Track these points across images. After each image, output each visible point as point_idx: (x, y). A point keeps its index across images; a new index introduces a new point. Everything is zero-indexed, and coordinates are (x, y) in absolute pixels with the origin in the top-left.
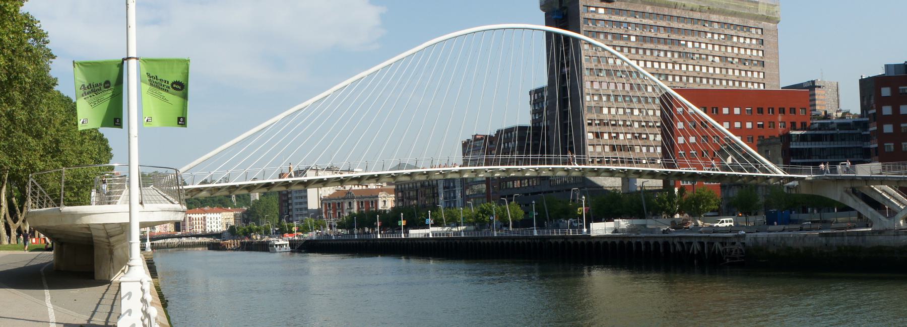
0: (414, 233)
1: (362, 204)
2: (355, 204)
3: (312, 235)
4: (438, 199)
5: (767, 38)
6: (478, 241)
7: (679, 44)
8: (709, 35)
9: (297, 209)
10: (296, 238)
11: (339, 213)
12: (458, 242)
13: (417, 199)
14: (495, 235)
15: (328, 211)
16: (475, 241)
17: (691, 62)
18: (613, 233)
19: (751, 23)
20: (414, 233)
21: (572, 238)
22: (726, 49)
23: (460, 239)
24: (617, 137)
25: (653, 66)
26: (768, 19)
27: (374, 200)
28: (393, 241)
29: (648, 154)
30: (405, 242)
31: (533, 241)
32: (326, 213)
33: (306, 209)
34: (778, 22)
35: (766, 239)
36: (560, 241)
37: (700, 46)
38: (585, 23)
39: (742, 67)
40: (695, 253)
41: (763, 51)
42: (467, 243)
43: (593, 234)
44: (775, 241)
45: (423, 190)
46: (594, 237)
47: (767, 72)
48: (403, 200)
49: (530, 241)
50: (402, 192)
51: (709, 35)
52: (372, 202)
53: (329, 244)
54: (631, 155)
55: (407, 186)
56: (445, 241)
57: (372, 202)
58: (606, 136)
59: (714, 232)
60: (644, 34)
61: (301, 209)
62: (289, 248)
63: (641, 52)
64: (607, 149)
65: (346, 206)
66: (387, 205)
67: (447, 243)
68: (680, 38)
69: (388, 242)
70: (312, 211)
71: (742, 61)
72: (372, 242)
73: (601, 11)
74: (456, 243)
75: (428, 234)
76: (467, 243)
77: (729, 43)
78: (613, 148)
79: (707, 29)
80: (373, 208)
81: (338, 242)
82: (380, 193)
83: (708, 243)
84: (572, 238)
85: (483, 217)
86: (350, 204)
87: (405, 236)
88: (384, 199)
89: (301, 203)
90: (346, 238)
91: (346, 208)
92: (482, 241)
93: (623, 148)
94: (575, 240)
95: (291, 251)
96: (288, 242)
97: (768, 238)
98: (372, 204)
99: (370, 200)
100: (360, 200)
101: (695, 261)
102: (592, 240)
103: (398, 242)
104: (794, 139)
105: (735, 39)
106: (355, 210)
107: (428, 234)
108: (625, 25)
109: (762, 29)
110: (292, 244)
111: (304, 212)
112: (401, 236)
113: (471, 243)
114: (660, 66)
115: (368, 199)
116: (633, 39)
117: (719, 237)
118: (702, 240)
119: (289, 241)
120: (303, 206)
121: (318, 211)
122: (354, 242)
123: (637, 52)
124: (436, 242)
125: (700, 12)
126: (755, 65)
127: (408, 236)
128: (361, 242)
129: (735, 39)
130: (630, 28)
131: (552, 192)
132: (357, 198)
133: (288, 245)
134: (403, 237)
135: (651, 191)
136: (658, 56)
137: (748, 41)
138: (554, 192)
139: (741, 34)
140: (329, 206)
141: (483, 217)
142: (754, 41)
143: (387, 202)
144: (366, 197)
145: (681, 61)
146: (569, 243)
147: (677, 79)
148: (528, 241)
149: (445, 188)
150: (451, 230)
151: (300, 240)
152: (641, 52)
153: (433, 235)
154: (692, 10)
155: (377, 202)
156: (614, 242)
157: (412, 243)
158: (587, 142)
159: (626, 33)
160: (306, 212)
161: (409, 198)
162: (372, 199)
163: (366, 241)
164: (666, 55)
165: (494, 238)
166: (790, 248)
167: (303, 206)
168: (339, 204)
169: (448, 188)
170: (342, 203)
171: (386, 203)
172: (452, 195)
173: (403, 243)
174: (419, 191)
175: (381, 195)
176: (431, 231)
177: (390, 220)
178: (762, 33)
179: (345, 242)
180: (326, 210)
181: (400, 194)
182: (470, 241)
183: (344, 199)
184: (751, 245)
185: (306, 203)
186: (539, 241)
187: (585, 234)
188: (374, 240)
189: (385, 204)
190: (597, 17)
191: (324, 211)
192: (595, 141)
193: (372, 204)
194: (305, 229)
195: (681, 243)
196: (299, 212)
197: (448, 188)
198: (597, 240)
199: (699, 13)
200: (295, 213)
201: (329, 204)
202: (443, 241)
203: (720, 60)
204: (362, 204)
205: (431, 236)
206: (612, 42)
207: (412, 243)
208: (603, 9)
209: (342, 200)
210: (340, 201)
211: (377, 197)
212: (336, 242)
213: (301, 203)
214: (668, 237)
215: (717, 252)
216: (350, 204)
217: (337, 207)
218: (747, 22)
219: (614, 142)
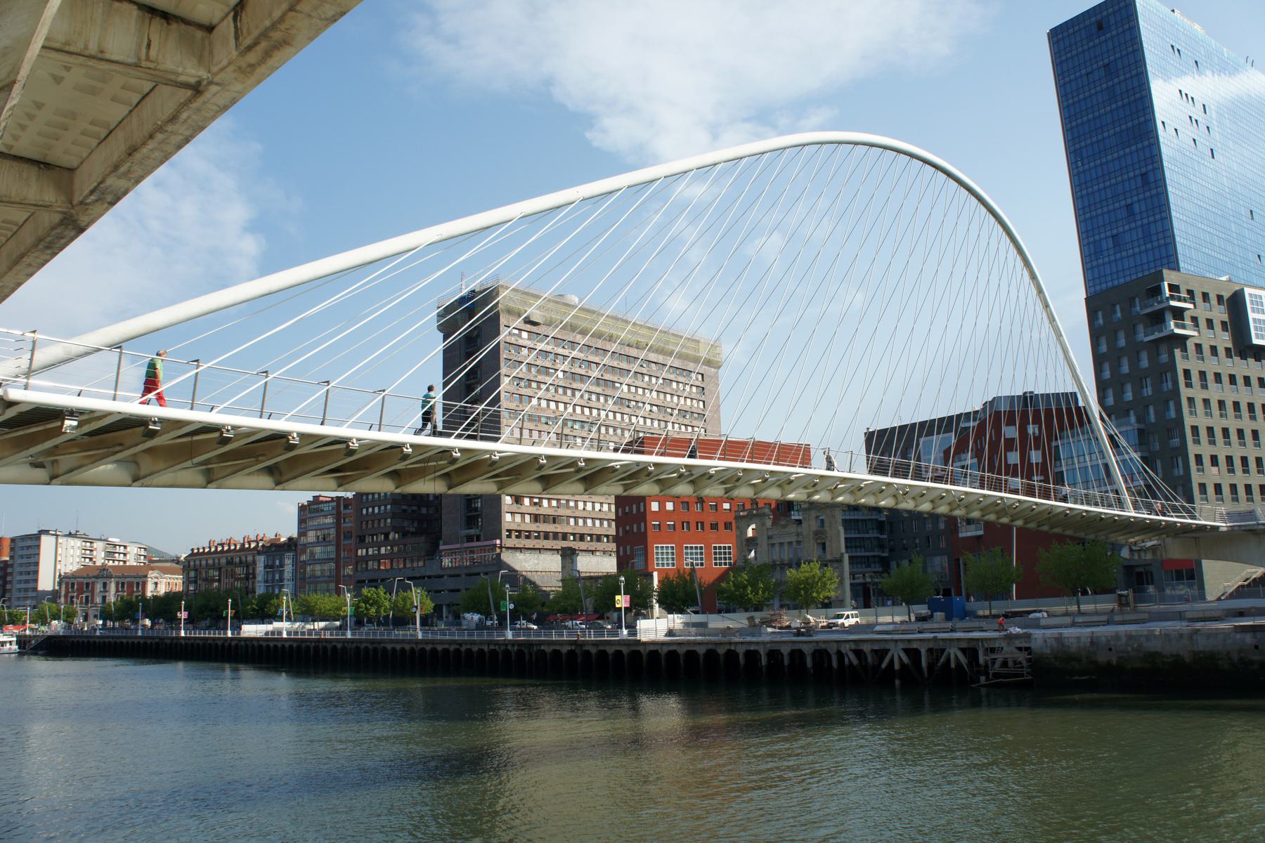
0: (251, 630)
1: (123, 587)
2: (113, 587)
3: (57, 626)
4: (253, 583)
5: (709, 387)
6: (382, 645)
7: (614, 387)
8: (647, 378)
9: (20, 590)
10: (28, 632)
11: (87, 597)
12: (339, 646)
13: (219, 581)
14: (420, 637)
15: (70, 595)
16: (375, 645)
17: (627, 410)
18: (666, 635)
19: (691, 366)
20: (251, 630)
21: (593, 645)
22: (665, 397)
23: (344, 642)
24: (539, 504)
25: (583, 412)
26: (708, 363)
27: (140, 580)
28: (209, 642)
29: (576, 527)
30: (233, 643)
31: (503, 648)
32: (66, 596)
33: (35, 589)
34: (719, 368)
35: (1089, 640)
36: (565, 649)
37: (636, 391)
38: (505, 348)
39: (681, 420)
40: (897, 666)
41: (704, 402)
42: (358, 648)
43: (643, 637)
44: (1112, 643)
45: (229, 569)
46: (645, 644)
47: (709, 428)
48: (196, 582)
49: (497, 647)
50: (196, 570)
51: (647, 378)
52: (138, 584)
53: (89, 642)
54: (559, 528)
55: (204, 563)
56: (313, 644)
57: (138, 584)
58: (527, 501)
59: (919, 632)
60: (573, 371)
61: (26, 590)
62: (15, 647)
63: (569, 392)
64: (527, 518)
65: (99, 587)
66: (158, 589)
67: (316, 648)
68: (615, 379)
69: (201, 642)
70: (45, 593)
71: (683, 412)
72: (168, 641)
73: (525, 335)
74: (335, 647)
75: (280, 633)
76: (358, 648)
77: (668, 390)
78: (536, 518)
79: (644, 371)
80: (138, 591)
81: (107, 640)
82: (150, 572)
83: (930, 651)
84: (593, 645)
85: (366, 608)
86: (105, 585)
87: (232, 634)
88: (156, 580)
89: (27, 581)
90: (120, 634)
91: (98, 590)
92: (389, 647)
93: (546, 519)
94: (601, 648)
95: (18, 653)
96: (15, 639)
97: (1092, 638)
98: (138, 587)
99: (135, 581)
100: (121, 580)
101: (897, 682)
102: (641, 649)
103: (220, 643)
104: (795, 508)
105: (674, 385)
106: (112, 598)
107: (280, 633)
108: (551, 356)
109: (702, 375)
110: (22, 642)
111: (31, 594)
112: (225, 633)
113: (367, 647)
114: (591, 413)
115: (132, 580)
116: (560, 375)
117: (958, 640)
118: (915, 646)
119: (17, 636)
120: (31, 585)
121: (54, 595)
122: (136, 641)
123: (565, 393)
124: (295, 645)
125: (638, 348)
126: (695, 419)
127: (239, 633)
128: (149, 641)
129: (674, 385)
130: (557, 361)
131: (441, 576)
132: (116, 577)
133: (14, 643)
134: (229, 634)
135: (591, 578)
136: (589, 399)
137: (688, 388)
138: (445, 577)
139: (681, 379)
140: (73, 587)
141: (366, 608)
142: (694, 389)
143: (161, 584)
144: (128, 577)
145: (616, 408)
146: (588, 652)
147: (611, 430)
148: (492, 647)
149: (266, 567)
150: (303, 627)
151: (35, 636)
152: (569, 392)
153: (289, 633)
154: (628, 345)
155: (144, 584)
156: (694, 652)
157: (246, 645)
158: (504, 508)
159: (553, 367)
160: (34, 594)
161: (209, 580)
162: (138, 580)
163: (157, 640)
164: (598, 399)
165: (417, 642)
166: (1153, 656)
167: (31, 585)
168: (88, 584)
169: (272, 567)
170: (93, 583)
171: (159, 586)
172: (277, 577)
173: (230, 644)
174: (223, 570)
175: (152, 574)
176: (283, 627)
177: (164, 607)
178: (703, 380)
179: (118, 641)
180: (67, 592)
181: (192, 574)
182: (364, 645)
183: (96, 577)
184: (1049, 652)
185: (36, 581)
186: (516, 648)
187: (625, 638)
188: (173, 638)
189: (156, 587)
190: (521, 342)
191: (63, 593)
192: (515, 508)
193: (138, 587)
194: (42, 619)
195: (858, 653)
196: (22, 595)
197: (272, 567)
198: (652, 648)
199: (636, 350)
200: (15, 594)
201: (73, 584)
202: (308, 644)
203: (659, 410)
204: (123, 587)
205: (285, 635)
206: (536, 377)
207: (246, 645)
208: (526, 333)
209: (93, 580)
210: (90, 581)
211: (146, 576)
212: (102, 640)
213: (27, 581)
214: (757, 643)
215: (953, 665)
216: (105, 585)
217: (135, 589)
218: (686, 365)
219: (534, 510)
